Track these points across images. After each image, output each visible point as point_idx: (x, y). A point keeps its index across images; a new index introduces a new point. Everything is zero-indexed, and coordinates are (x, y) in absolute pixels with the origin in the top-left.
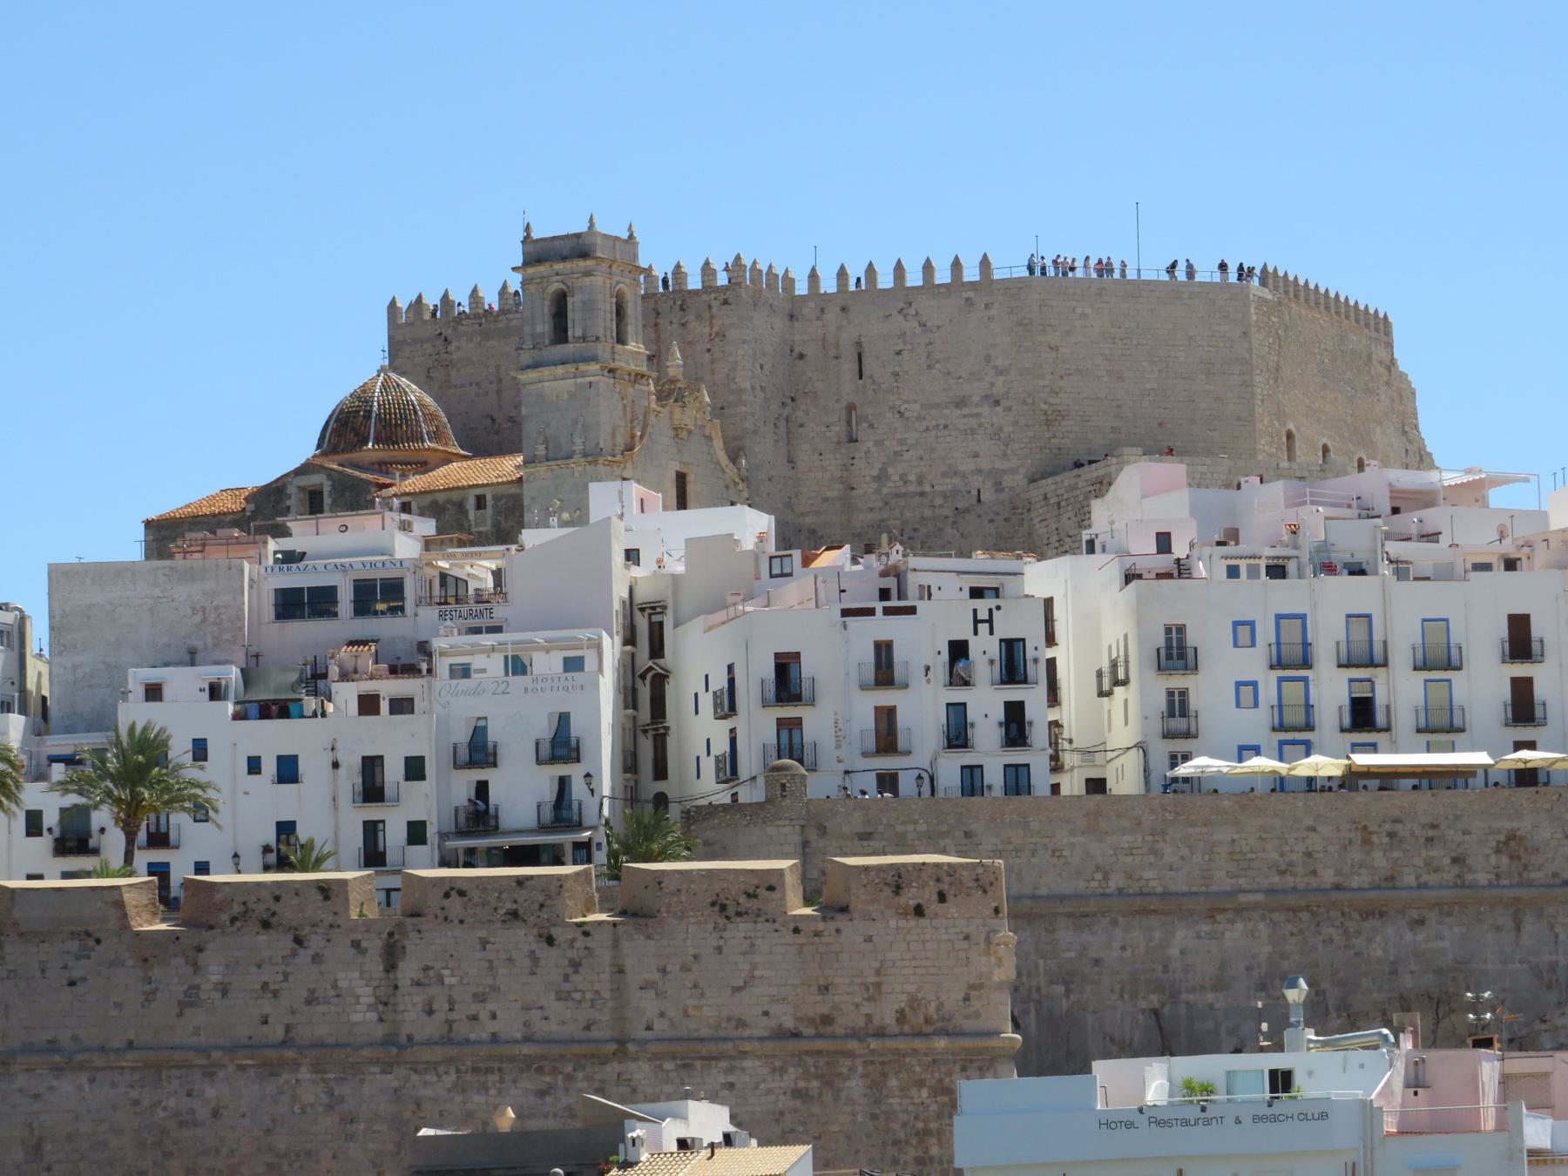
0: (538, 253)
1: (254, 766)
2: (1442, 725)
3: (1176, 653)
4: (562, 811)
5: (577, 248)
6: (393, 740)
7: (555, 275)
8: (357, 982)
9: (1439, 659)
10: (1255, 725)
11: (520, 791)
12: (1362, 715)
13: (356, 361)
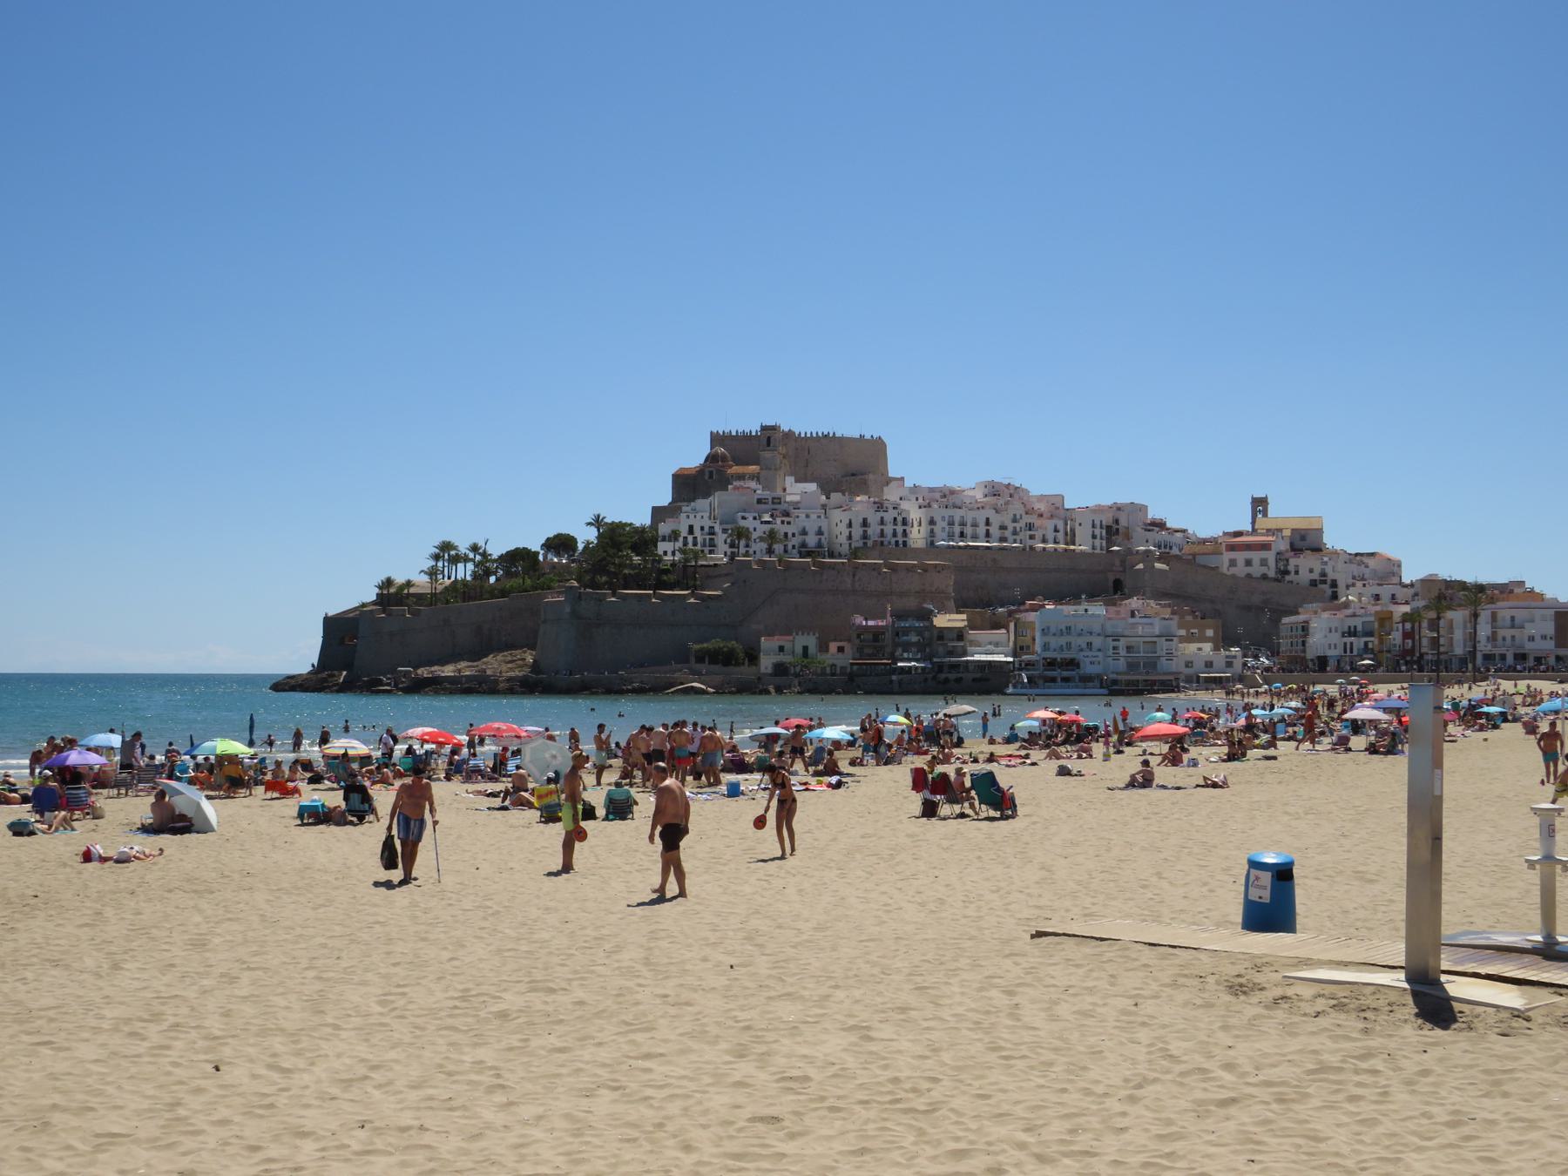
0: (764, 428)
2: (975, 537)
3: (932, 522)
4: (819, 545)
5: (774, 428)
6: (790, 530)
7: (768, 433)
8: (849, 580)
9: (975, 525)
10: (945, 535)
12: (962, 535)
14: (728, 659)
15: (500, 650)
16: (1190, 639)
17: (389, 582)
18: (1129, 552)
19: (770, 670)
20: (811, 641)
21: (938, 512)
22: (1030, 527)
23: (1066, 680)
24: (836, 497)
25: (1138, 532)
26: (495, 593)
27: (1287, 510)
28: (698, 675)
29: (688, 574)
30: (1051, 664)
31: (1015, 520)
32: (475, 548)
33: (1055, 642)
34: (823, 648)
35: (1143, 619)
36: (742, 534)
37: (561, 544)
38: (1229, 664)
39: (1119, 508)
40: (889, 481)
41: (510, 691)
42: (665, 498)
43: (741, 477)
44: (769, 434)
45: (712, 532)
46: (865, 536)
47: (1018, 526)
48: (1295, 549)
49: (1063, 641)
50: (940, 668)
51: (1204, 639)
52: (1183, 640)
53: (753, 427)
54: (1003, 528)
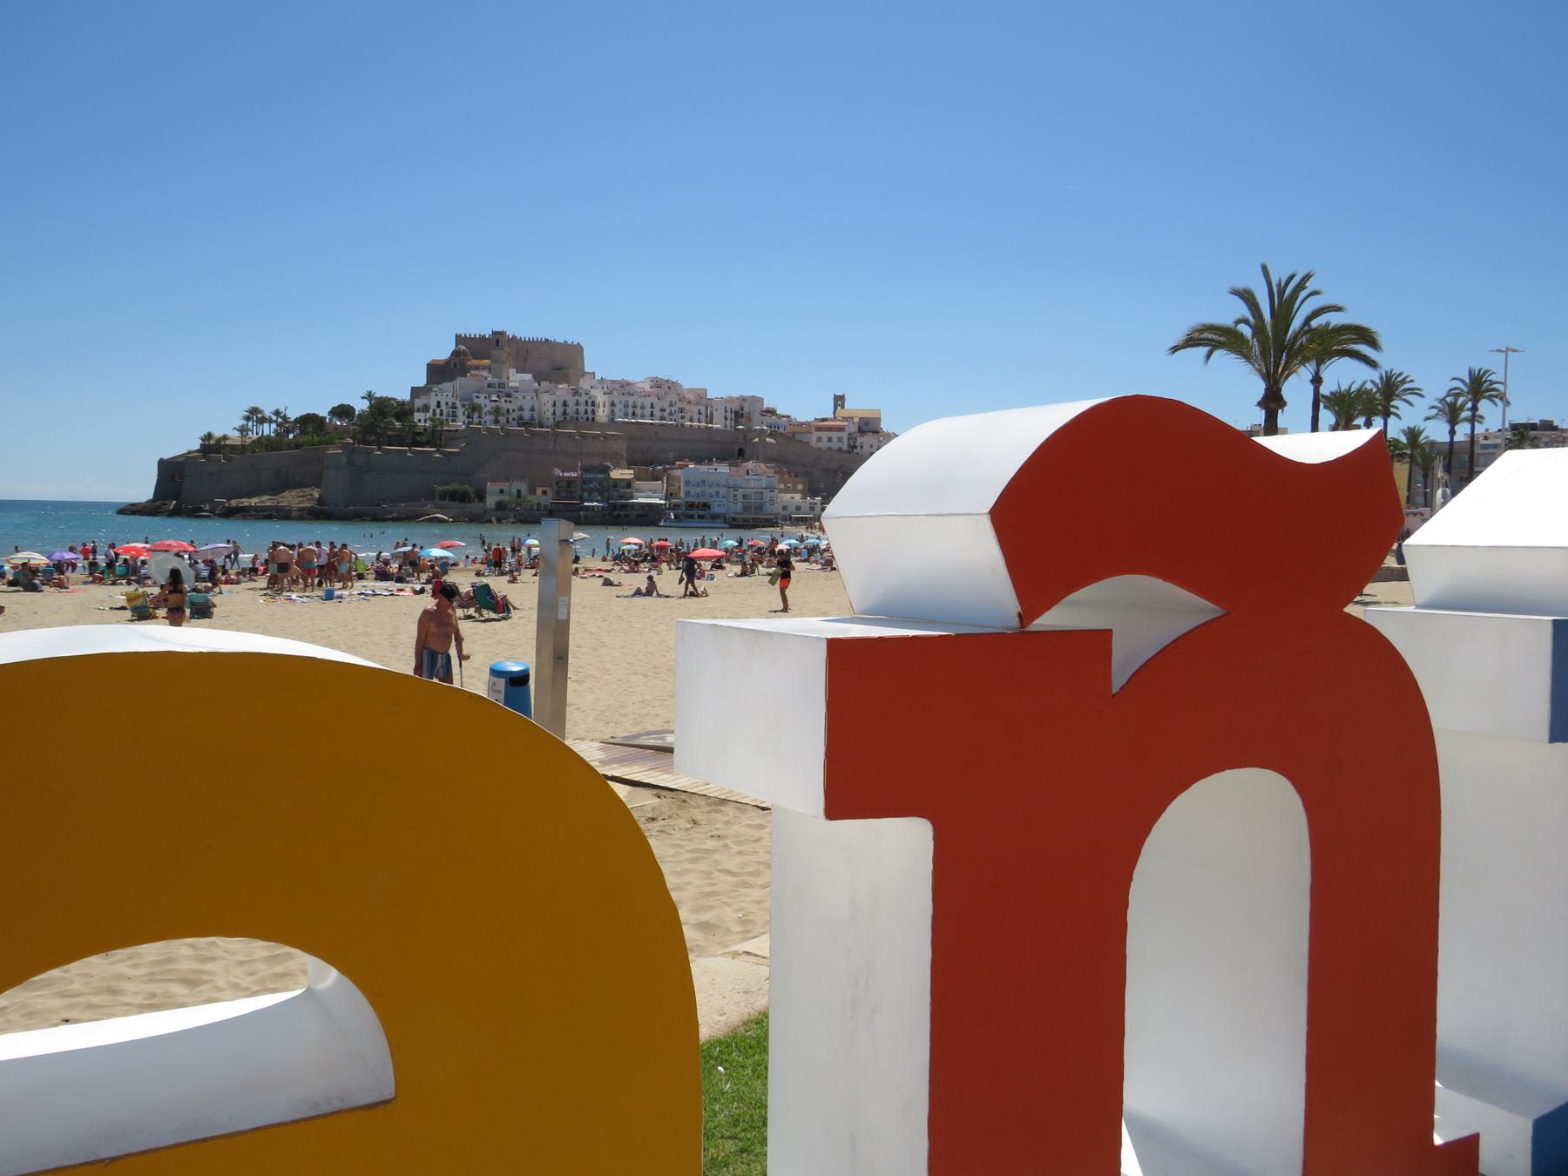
0: (494, 333)
2: (643, 417)
3: (613, 404)
4: (532, 418)
5: (501, 333)
9: (643, 408)
14: (462, 497)
15: (294, 487)
16: (787, 490)
17: (209, 436)
18: (750, 430)
20: (523, 486)
21: (617, 398)
22: (682, 410)
23: (700, 517)
24: (545, 384)
25: (756, 417)
26: (290, 446)
27: (857, 405)
28: (441, 509)
29: (435, 436)
30: (691, 506)
32: (277, 413)
33: (693, 490)
34: (532, 491)
35: (756, 475)
36: (475, 408)
37: (343, 411)
38: (812, 509)
39: (744, 399)
40: (584, 374)
41: (301, 518)
42: (422, 381)
43: (477, 368)
44: (498, 338)
45: (454, 407)
46: (565, 413)
48: (862, 431)
49: (699, 490)
50: (614, 507)
51: (797, 492)
52: (781, 491)
53: (483, 329)
54: (663, 410)
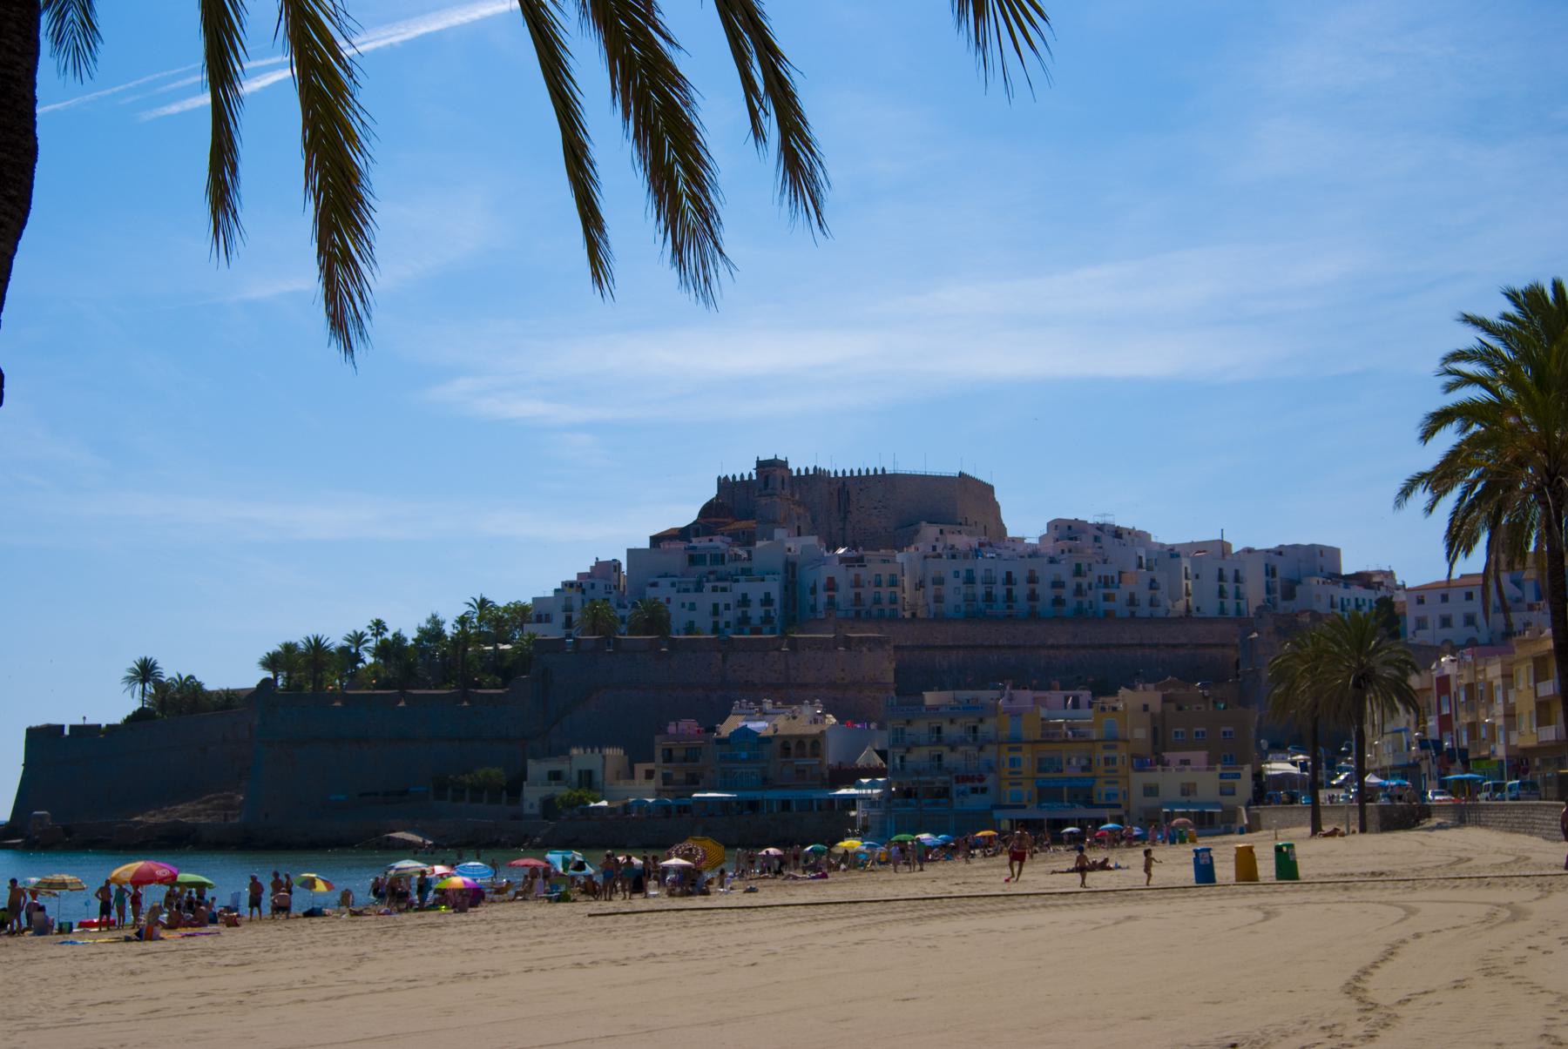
0: (762, 465)
1: (683, 605)
4: (767, 619)
11: (756, 612)
13: (711, 492)
19: (536, 810)
31: (1078, 571)
47: (1084, 582)
